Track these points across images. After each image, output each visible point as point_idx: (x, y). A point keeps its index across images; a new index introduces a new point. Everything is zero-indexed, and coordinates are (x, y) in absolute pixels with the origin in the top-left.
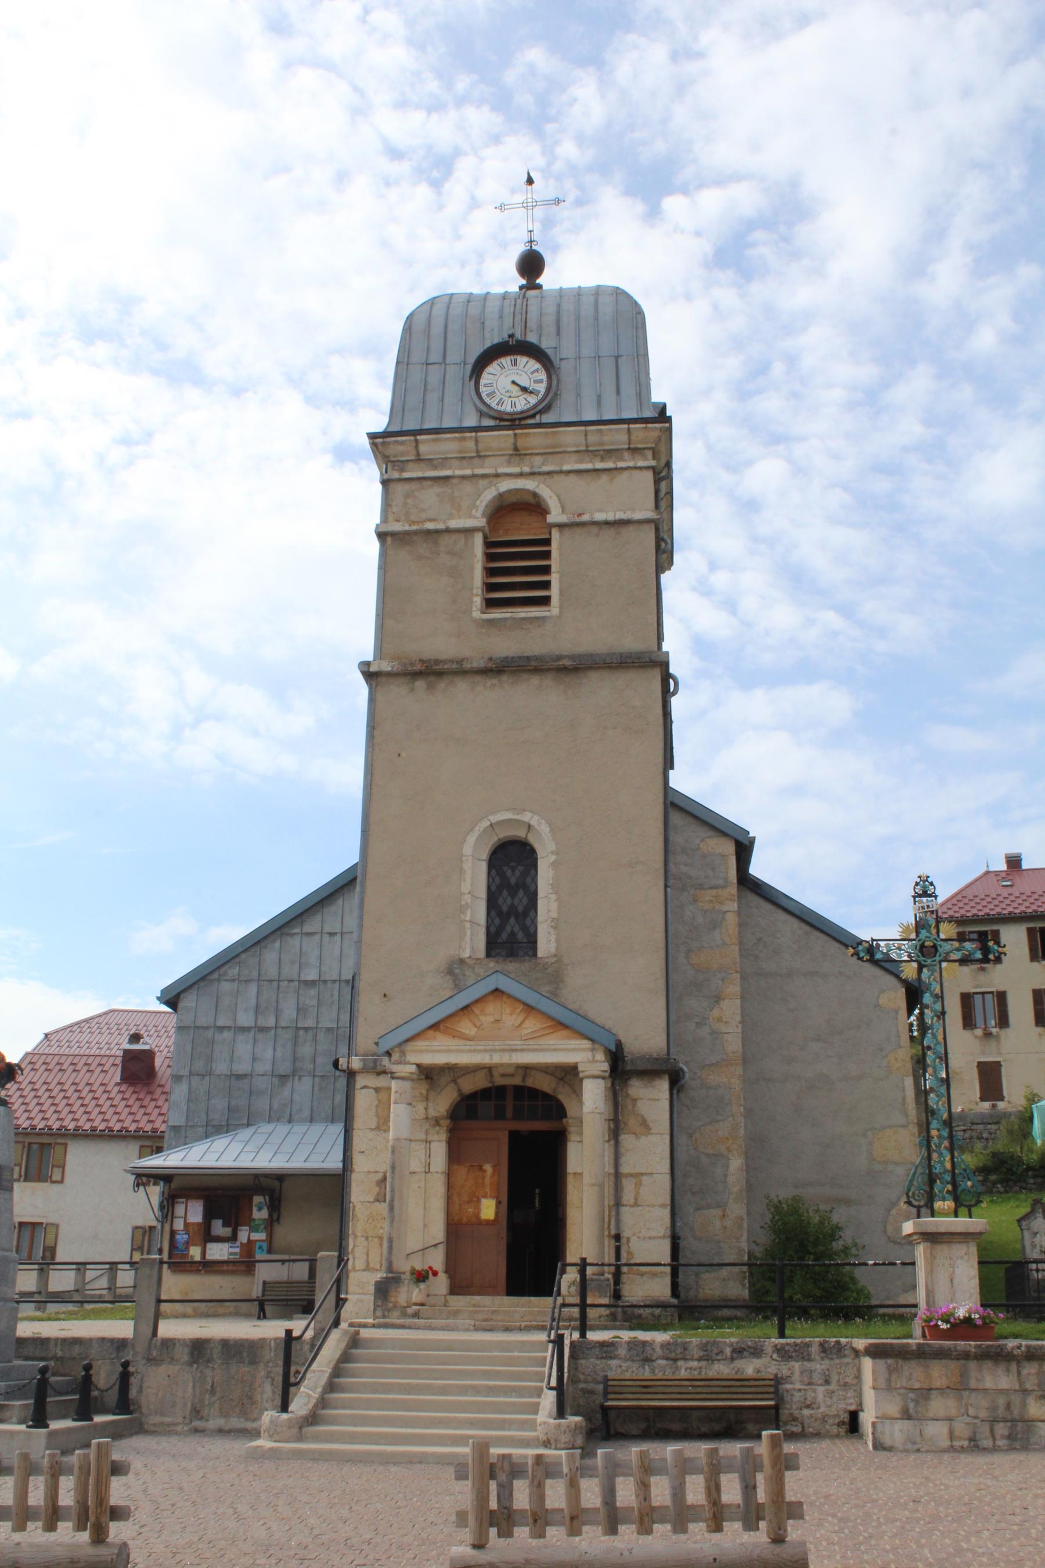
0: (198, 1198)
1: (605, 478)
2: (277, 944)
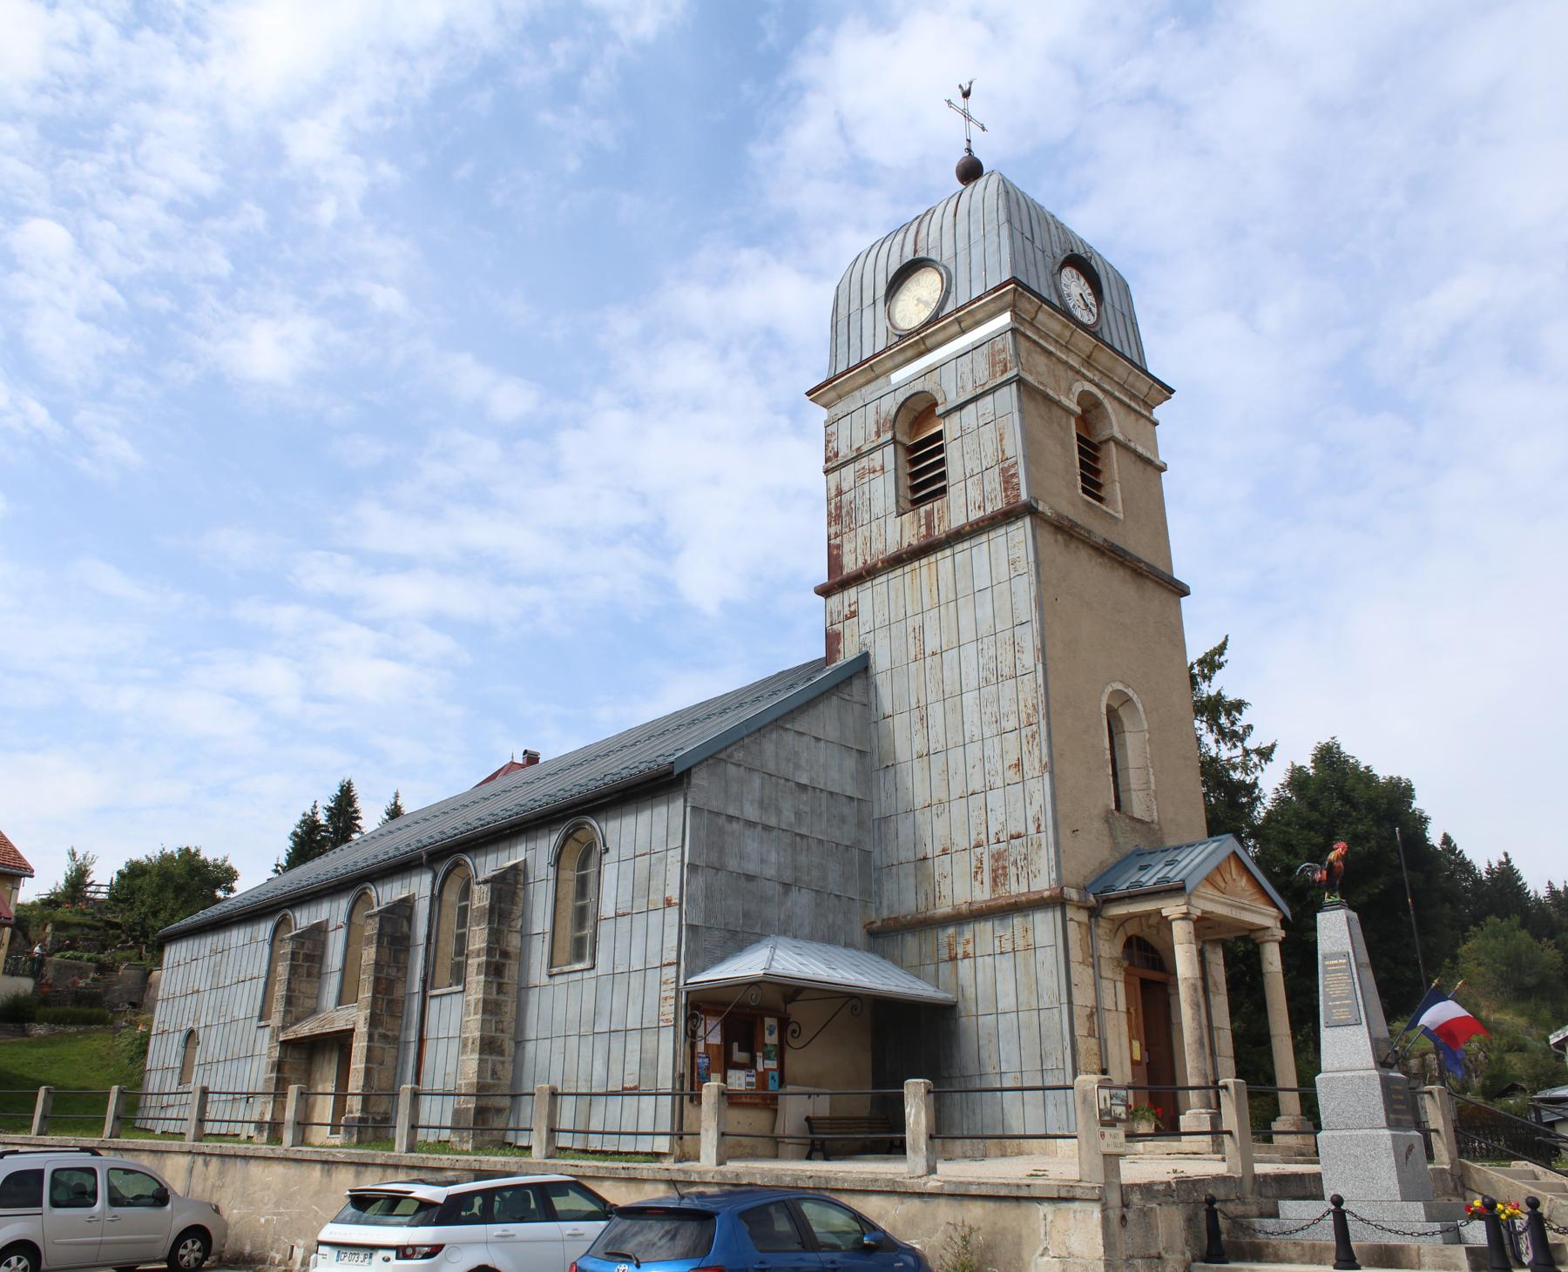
0: (716, 1013)
1: (1133, 417)
2: (774, 736)
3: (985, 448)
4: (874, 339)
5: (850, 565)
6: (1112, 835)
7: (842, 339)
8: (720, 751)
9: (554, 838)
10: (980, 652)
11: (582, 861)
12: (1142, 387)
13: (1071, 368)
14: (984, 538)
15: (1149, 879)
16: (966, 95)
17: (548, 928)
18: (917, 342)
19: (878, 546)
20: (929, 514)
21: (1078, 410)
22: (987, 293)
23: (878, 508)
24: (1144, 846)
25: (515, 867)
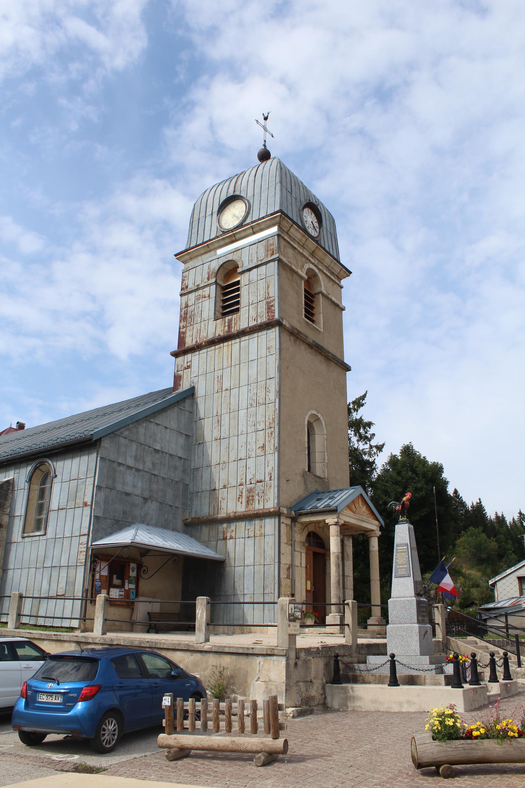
0: (106, 560)
2: (144, 425)
3: (259, 291)
4: (210, 232)
5: (189, 342)
6: (305, 484)
7: (195, 230)
8: (117, 430)
9: (29, 468)
10: (249, 391)
11: (42, 482)
12: (337, 269)
13: (304, 256)
14: (256, 335)
15: (321, 505)
16: (266, 119)
17: (23, 513)
18: (231, 236)
19: (204, 334)
20: (230, 321)
21: (306, 277)
22: (267, 216)
23: (205, 315)
24: (320, 489)
25: (8, 482)
